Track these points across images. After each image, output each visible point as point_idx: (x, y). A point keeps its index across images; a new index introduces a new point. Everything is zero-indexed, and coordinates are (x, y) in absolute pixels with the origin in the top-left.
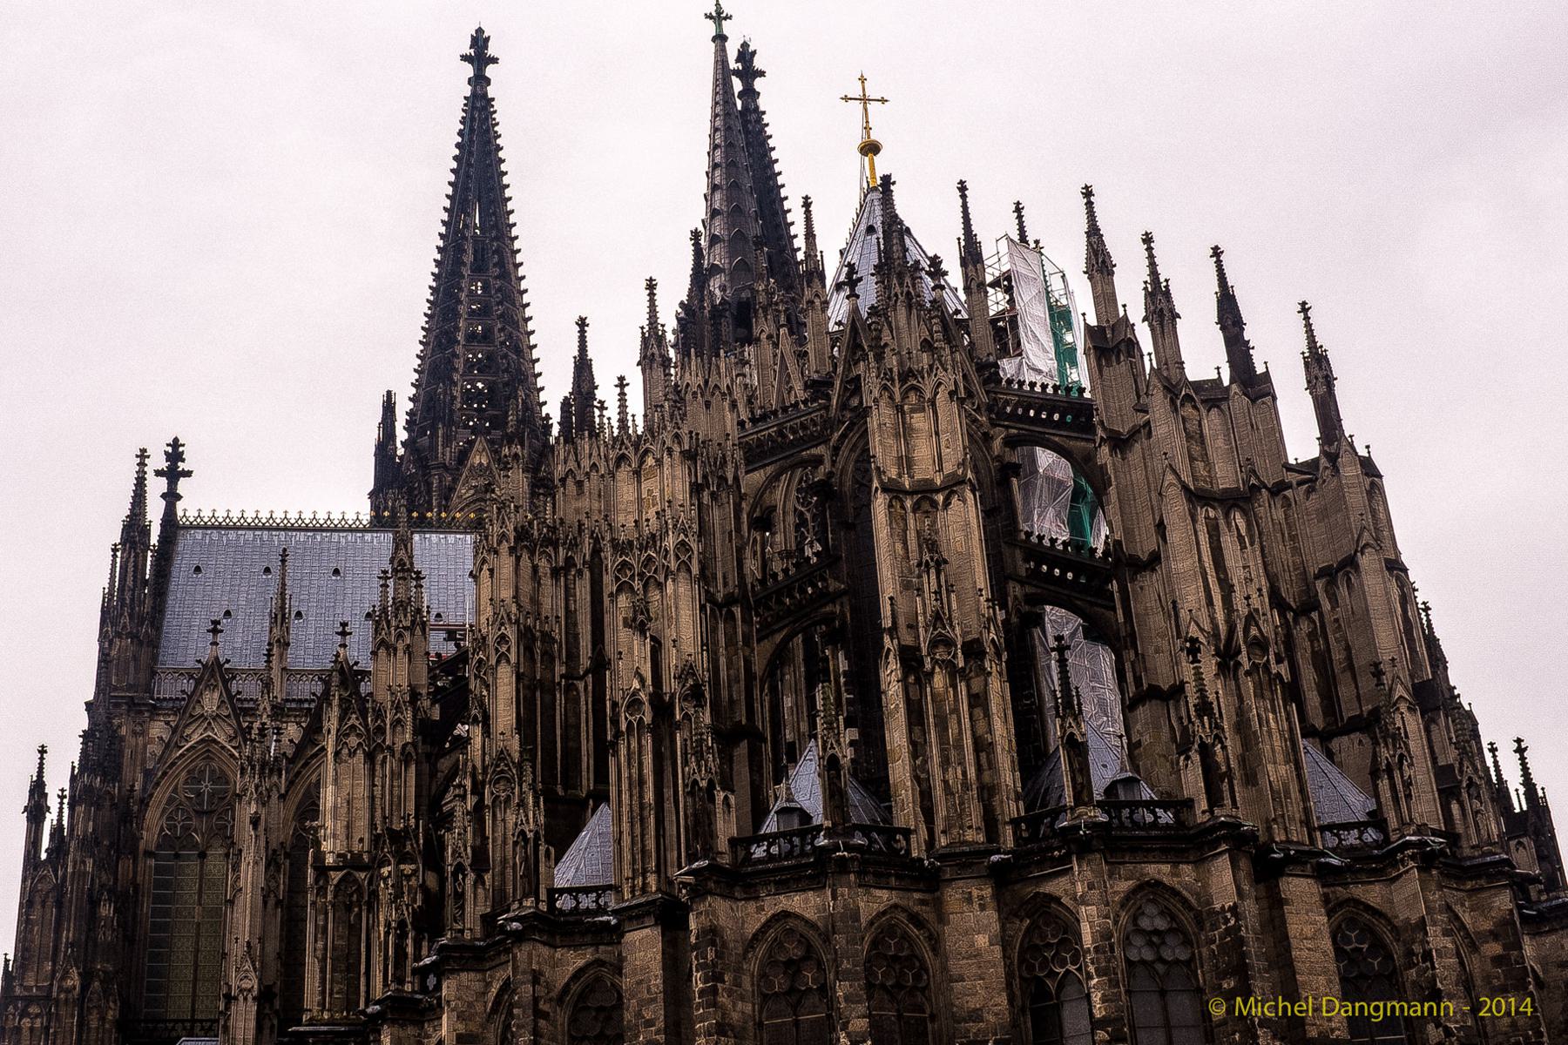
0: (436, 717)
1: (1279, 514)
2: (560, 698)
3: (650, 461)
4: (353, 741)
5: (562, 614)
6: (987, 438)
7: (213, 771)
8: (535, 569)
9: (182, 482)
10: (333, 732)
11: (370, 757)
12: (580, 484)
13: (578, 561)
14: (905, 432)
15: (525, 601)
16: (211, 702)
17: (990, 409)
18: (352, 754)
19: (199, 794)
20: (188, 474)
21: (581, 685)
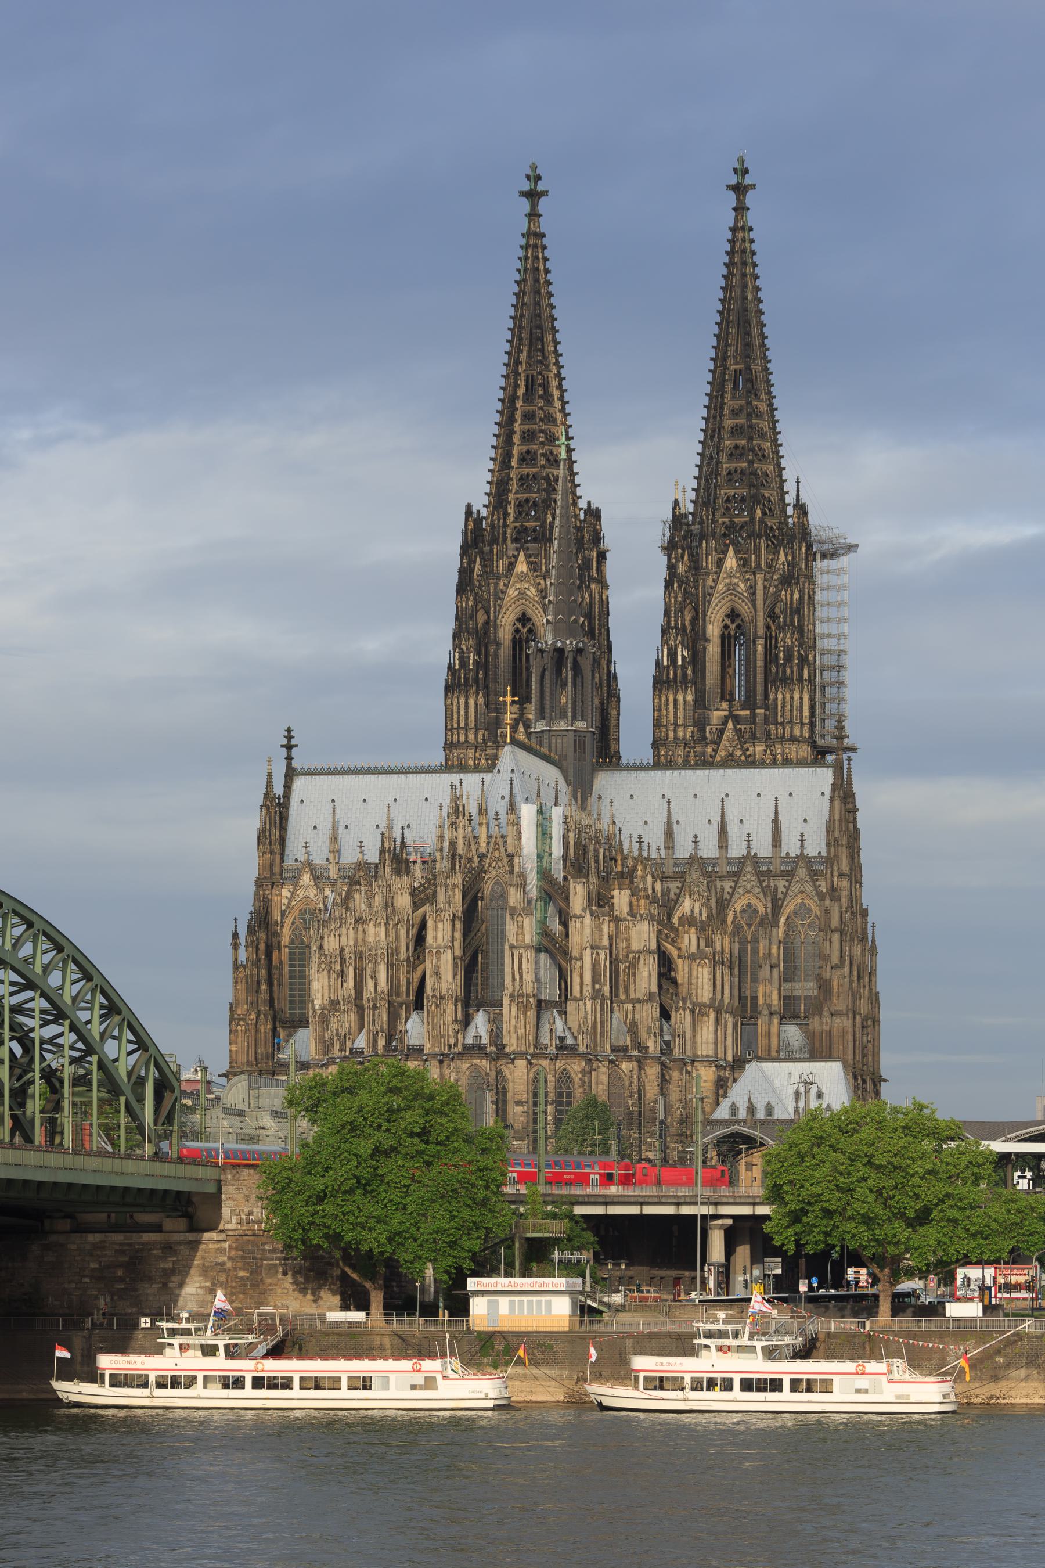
1: (578, 925)
4: (323, 966)
9: (294, 749)
11: (329, 972)
14: (436, 928)
16: (306, 878)
20: (296, 746)
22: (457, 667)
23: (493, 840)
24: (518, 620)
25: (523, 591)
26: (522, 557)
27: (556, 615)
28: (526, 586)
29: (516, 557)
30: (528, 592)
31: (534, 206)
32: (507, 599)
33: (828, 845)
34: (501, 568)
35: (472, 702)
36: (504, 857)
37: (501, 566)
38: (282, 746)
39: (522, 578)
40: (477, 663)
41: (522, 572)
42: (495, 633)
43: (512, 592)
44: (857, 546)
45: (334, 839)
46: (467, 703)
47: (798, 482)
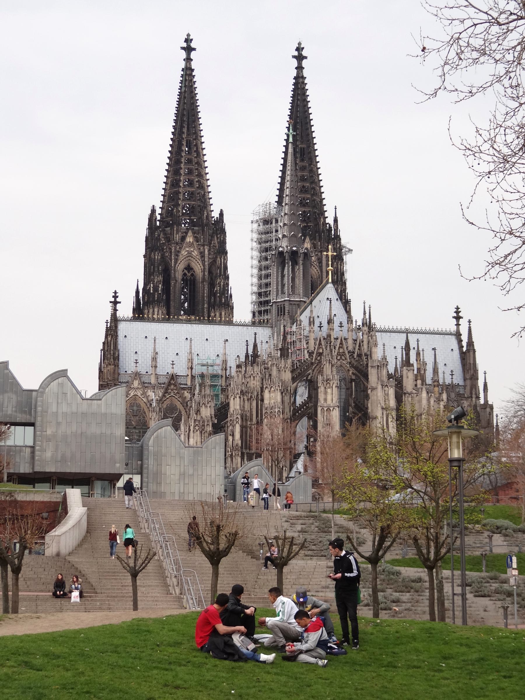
0: (216, 422)
1: (410, 399)
2: (248, 429)
3: (272, 389)
4: (197, 428)
5: (249, 409)
6: (348, 370)
7: (137, 404)
8: (244, 399)
9: (118, 305)
10: (193, 425)
11: (201, 432)
12: (254, 377)
13: (253, 396)
14: (326, 393)
15: (241, 407)
16: (136, 384)
17: (350, 363)
18: (197, 431)
19: (133, 410)
20: (120, 303)
21: (253, 426)
22: (152, 292)
23: (339, 340)
24: (185, 268)
25: (189, 255)
26: (190, 233)
27: (290, 232)
28: (192, 249)
29: (186, 233)
30: (193, 253)
31: (188, 54)
32: (181, 256)
33: (465, 380)
34: (177, 239)
35: (160, 312)
36: (347, 353)
37: (177, 237)
38: (111, 302)
39: (191, 245)
40: (163, 290)
41: (190, 242)
42: (175, 274)
43: (184, 253)
44: (352, 250)
45: (154, 359)
46: (158, 311)
47: (336, 208)
